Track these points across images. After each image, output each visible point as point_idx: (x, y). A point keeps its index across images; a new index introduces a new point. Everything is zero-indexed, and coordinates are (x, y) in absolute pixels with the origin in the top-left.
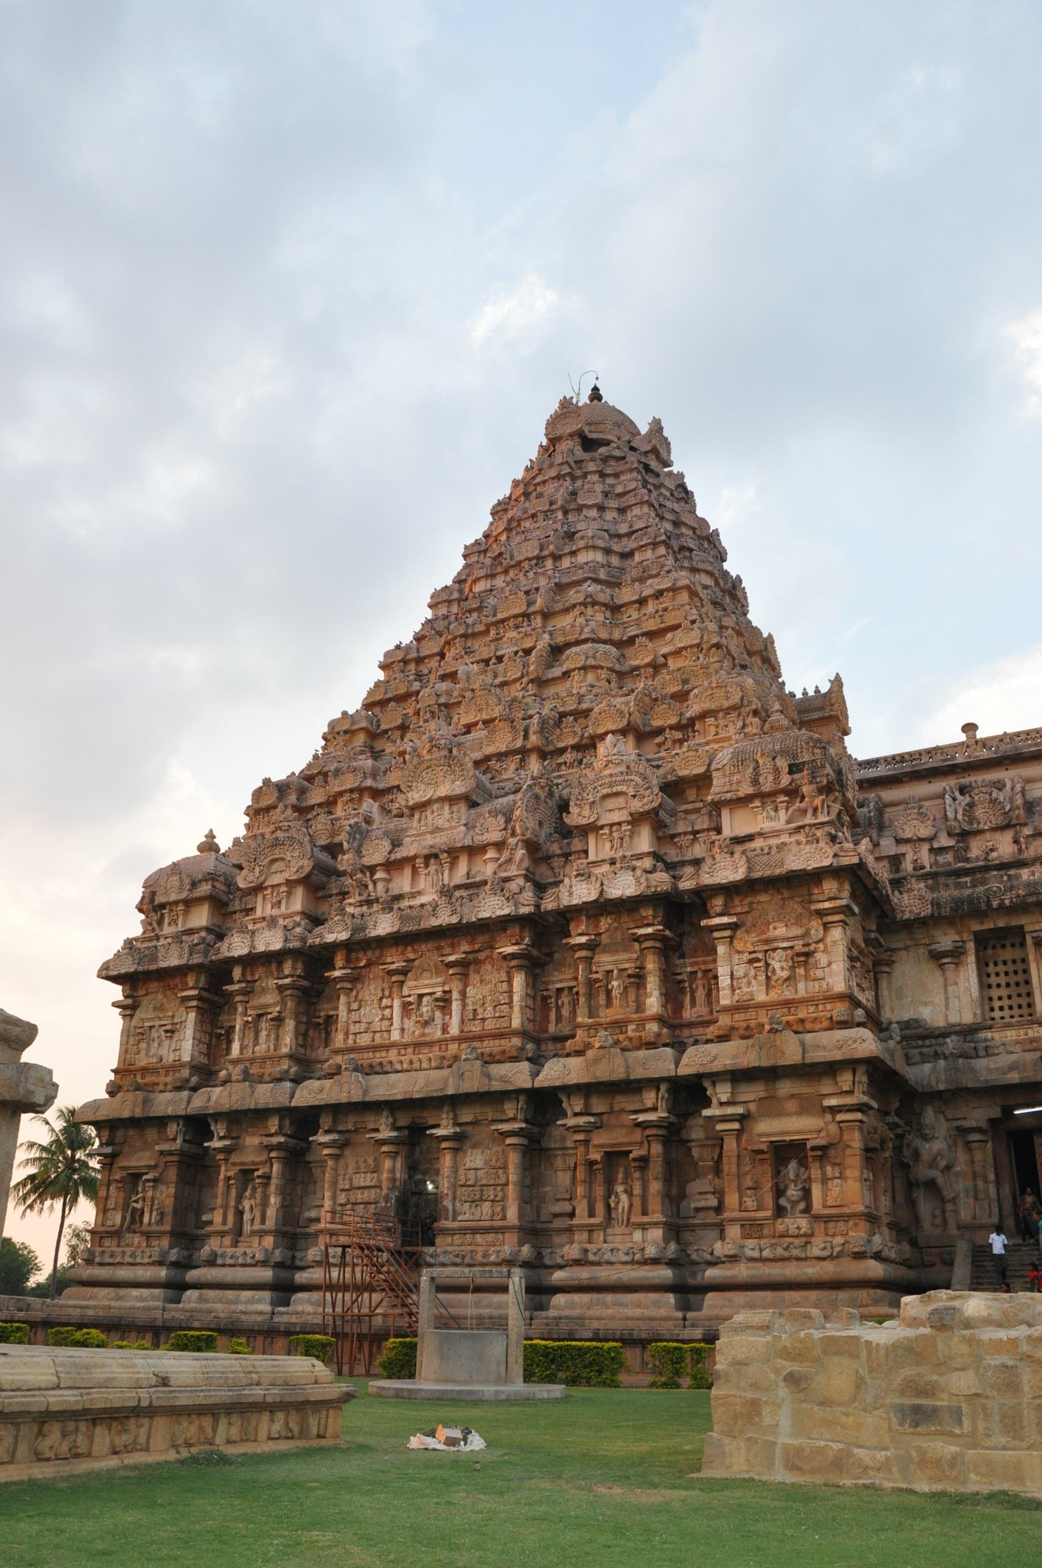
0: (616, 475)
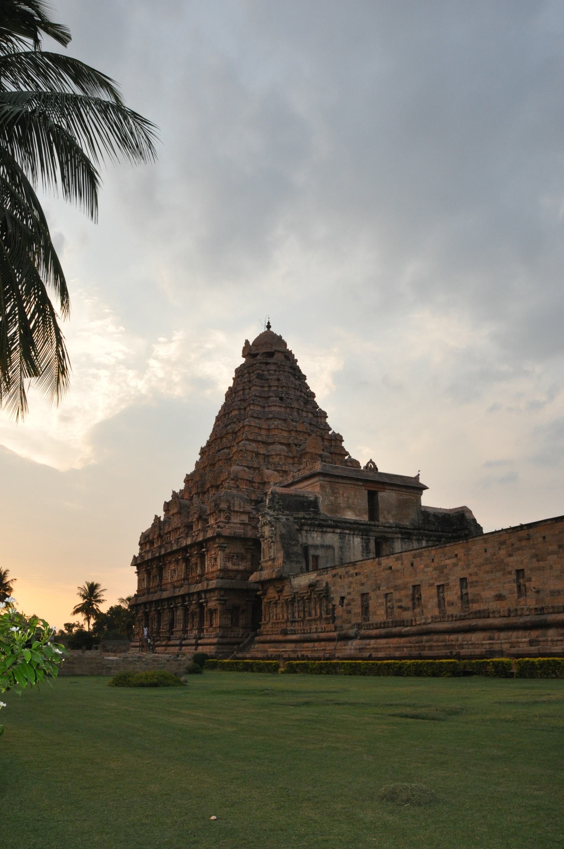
0: (253, 372)
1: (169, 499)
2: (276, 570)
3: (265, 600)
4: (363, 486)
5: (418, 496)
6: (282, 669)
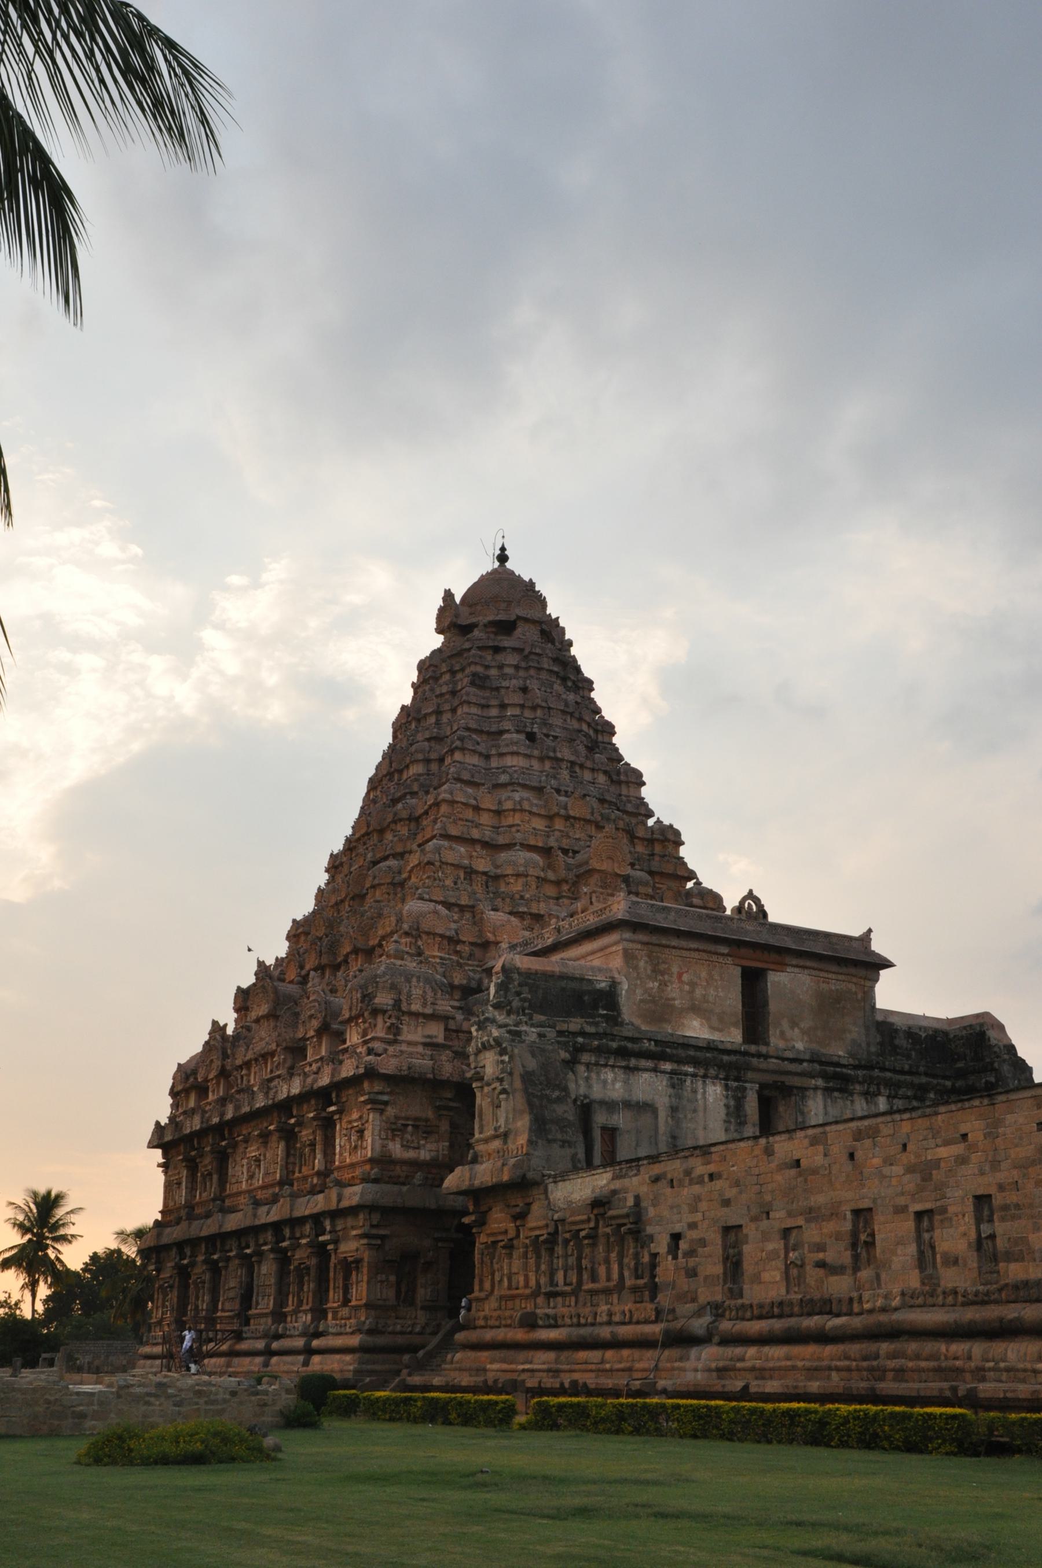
0: (463, 670)
1: (248, 980)
2: (512, 1161)
3: (483, 1238)
4: (728, 955)
5: (868, 984)
6: (521, 1419)
